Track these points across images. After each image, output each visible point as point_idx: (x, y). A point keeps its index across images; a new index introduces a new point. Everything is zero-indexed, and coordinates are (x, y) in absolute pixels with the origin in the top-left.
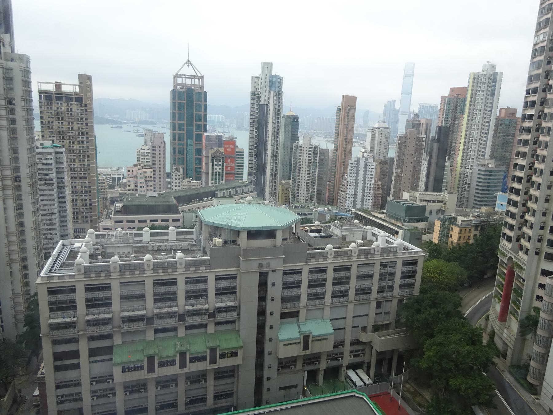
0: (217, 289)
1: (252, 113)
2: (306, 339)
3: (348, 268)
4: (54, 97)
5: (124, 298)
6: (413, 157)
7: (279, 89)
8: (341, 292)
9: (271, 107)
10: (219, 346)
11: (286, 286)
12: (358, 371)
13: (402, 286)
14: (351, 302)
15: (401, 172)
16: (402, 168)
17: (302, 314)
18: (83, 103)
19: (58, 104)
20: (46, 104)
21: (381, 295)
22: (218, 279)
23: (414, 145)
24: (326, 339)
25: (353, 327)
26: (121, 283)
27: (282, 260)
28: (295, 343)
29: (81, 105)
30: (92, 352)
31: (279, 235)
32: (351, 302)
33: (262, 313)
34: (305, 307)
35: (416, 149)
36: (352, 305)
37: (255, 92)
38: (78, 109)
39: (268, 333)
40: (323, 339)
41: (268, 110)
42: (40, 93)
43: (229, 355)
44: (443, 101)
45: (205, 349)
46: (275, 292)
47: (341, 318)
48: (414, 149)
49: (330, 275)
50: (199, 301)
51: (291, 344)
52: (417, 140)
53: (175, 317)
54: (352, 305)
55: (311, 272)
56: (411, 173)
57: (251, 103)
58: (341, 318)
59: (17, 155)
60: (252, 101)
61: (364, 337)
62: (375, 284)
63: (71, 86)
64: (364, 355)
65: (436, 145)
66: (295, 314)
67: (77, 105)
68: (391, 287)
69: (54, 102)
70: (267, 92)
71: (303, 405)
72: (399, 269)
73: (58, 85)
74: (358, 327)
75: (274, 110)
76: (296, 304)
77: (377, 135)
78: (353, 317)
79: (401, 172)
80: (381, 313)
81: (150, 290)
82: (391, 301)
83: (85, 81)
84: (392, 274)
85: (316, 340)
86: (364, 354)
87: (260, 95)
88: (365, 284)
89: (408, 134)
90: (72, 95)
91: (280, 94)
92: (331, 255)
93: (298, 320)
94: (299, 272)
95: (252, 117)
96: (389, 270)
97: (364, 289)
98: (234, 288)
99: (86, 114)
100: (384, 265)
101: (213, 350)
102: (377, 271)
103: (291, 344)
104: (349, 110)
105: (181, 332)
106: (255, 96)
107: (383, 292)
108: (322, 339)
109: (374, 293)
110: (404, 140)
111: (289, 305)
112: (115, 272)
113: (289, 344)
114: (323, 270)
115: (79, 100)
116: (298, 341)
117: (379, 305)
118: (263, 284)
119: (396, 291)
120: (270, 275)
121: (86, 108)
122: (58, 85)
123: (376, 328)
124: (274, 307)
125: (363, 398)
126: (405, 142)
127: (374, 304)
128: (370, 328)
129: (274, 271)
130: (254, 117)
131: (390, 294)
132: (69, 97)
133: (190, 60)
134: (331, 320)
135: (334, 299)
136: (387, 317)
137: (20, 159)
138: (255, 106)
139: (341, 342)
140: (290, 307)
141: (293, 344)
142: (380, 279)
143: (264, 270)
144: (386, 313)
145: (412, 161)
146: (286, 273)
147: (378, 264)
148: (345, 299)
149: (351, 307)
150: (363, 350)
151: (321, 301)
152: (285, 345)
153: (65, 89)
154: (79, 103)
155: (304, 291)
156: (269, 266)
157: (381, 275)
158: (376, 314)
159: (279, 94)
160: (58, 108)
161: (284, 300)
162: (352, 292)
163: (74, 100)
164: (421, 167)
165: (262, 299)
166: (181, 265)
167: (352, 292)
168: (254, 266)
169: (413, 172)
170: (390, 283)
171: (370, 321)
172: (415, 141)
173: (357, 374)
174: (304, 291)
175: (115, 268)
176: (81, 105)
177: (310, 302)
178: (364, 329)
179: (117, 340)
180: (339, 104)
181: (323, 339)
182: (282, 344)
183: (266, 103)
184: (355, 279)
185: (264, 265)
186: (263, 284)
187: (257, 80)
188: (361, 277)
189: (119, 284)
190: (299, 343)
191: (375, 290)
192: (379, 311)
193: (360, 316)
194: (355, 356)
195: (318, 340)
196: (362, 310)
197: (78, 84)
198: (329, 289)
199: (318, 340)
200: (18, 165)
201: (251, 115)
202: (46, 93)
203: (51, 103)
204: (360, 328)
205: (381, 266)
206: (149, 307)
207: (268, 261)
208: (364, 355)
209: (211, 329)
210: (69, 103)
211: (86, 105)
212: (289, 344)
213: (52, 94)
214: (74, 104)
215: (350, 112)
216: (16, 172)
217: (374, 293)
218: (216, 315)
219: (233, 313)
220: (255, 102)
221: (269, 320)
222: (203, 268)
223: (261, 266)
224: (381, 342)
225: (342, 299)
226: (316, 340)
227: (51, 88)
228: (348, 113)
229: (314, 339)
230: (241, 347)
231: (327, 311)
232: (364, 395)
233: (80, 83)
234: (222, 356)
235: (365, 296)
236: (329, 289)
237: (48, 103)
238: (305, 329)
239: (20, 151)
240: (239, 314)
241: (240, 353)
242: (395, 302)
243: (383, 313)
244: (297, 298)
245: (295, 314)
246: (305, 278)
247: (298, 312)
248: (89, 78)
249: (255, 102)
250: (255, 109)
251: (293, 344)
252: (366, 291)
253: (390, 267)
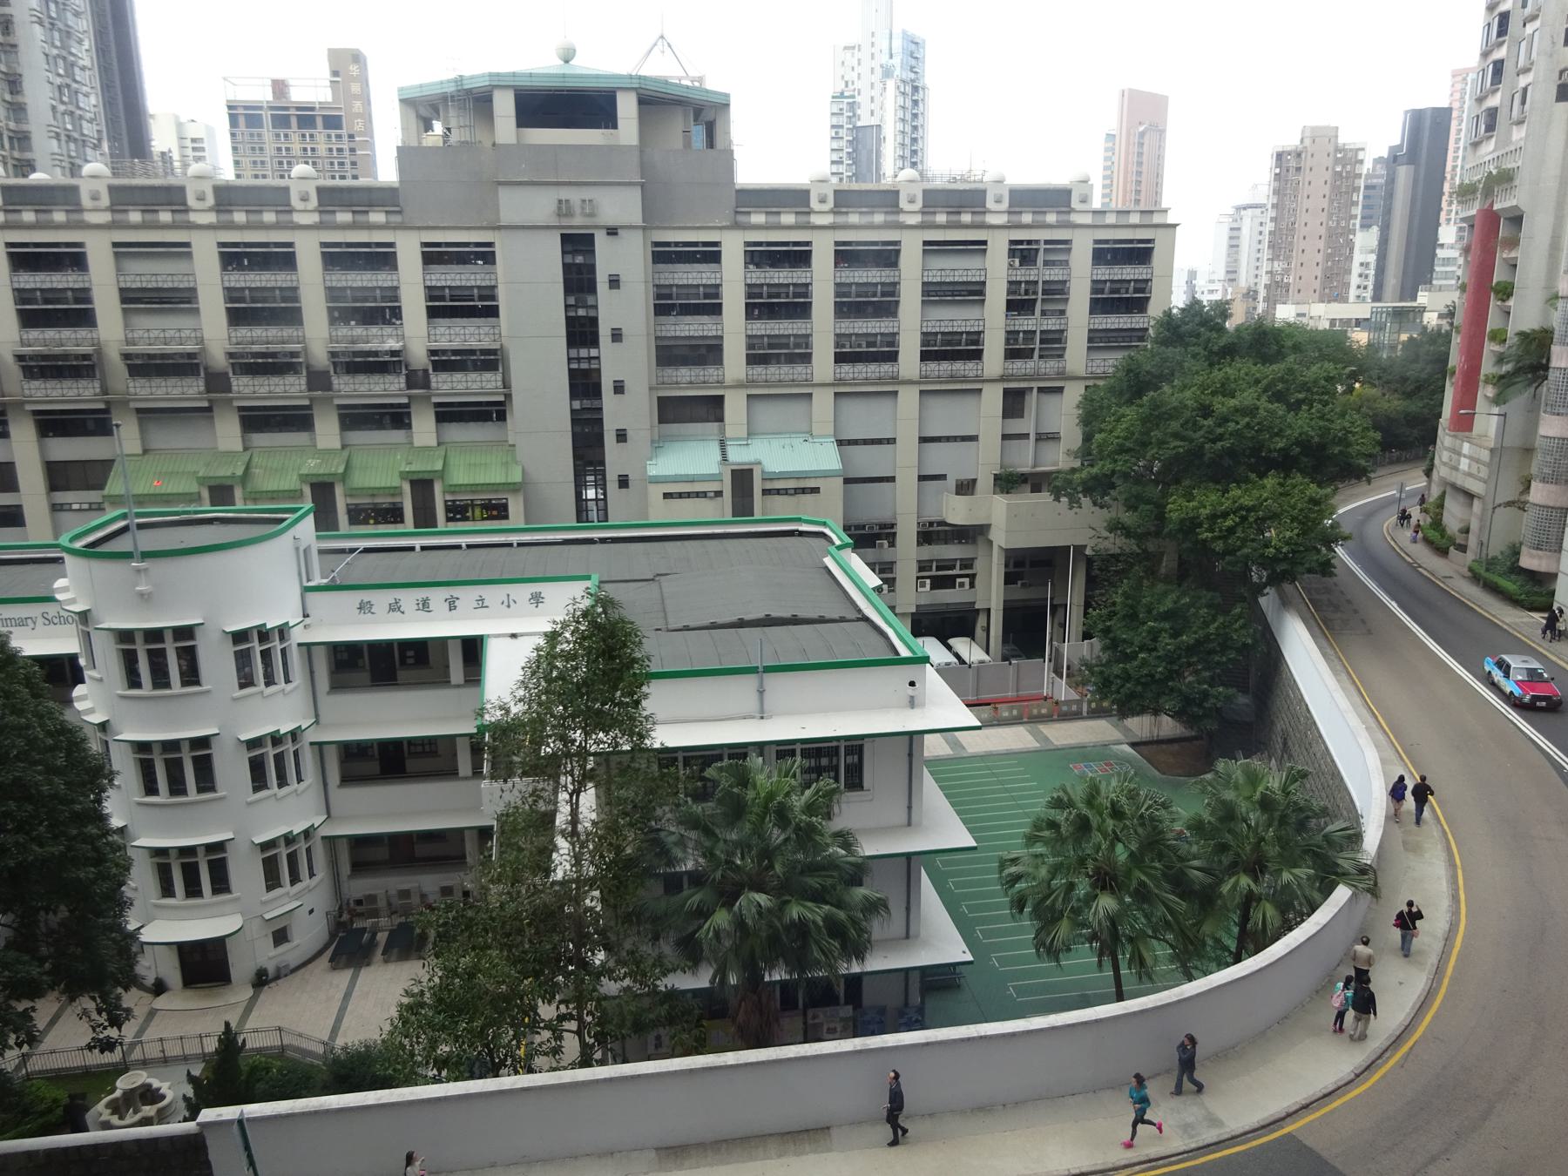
0: (432, 293)
1: (835, 158)
2: (742, 478)
3: (888, 257)
4: (267, 116)
5: (130, 298)
6: (1324, 217)
7: (913, 76)
8: (870, 339)
9: (890, 131)
10: (442, 474)
11: (666, 304)
12: (951, 641)
13: (1097, 340)
14: (910, 382)
15: (1287, 271)
16: (1288, 259)
17: (735, 406)
18: (344, 132)
19: (278, 136)
20: (247, 138)
21: (1019, 366)
22: (433, 256)
23: (1328, 176)
24: (816, 490)
25: (922, 478)
26: (115, 245)
27: (636, 195)
28: (704, 495)
29: (339, 137)
30: (59, 476)
31: (627, 107)
32: (910, 382)
33: (584, 384)
34: (739, 385)
35: (1335, 189)
36: (915, 390)
37: (842, 95)
38: (330, 150)
39: (615, 458)
40: (804, 491)
41: (880, 141)
42: (230, 107)
43: (478, 512)
44: (1459, 86)
45: (396, 482)
46: (624, 308)
47: (879, 442)
48: (1327, 190)
49: (823, 278)
50: (374, 330)
51: (689, 495)
52: (1337, 161)
53: (296, 372)
54: (915, 390)
55: (758, 257)
56: (1319, 272)
57: (833, 127)
58: (879, 442)
59: (19, 99)
60: (835, 121)
61: (957, 511)
62: (993, 320)
63: (312, 89)
64: (972, 585)
65: (1403, 172)
66: (712, 408)
67: (329, 136)
68: (1054, 342)
69: (267, 132)
70: (879, 86)
71: (603, 541)
72: (1081, 274)
73: (279, 87)
74: (942, 477)
75: (899, 139)
76: (711, 372)
77: (1245, 231)
78: (924, 440)
79: (1287, 271)
80: (1026, 436)
81: (209, 280)
82: (1060, 390)
83: (347, 66)
84: (1057, 291)
85: (778, 492)
86: (972, 577)
87: (858, 99)
88: (954, 318)
89: (1307, 142)
90: (312, 109)
91: (915, 89)
92: (823, 201)
93: (722, 431)
94: (711, 255)
95: (835, 169)
96: (1040, 273)
97: (952, 337)
98: (489, 293)
99: (354, 164)
100: (1023, 253)
101: (422, 486)
102: (997, 271)
103: (689, 495)
104: (1142, 134)
105: (327, 431)
106: (845, 102)
107: (1026, 354)
108: (803, 487)
109: (993, 358)
110: (1293, 164)
111: (685, 373)
112: (96, 210)
113: (680, 495)
114: (799, 257)
115: (333, 122)
116: (715, 487)
117: (1014, 403)
118: (579, 280)
119: (1076, 355)
120: (601, 242)
121: (352, 145)
122: (279, 87)
123: (1007, 482)
124: (626, 362)
125: (823, 535)
126: (1298, 169)
127: (993, 398)
128: (985, 483)
129: (612, 231)
130: (842, 168)
131: (1050, 366)
132: (306, 118)
133: (670, 38)
134: (840, 443)
135: (847, 370)
136: (1048, 447)
137: (31, 110)
138: (843, 132)
139: (883, 526)
140: (687, 381)
141: (698, 495)
142: (1012, 306)
143: (578, 222)
144: (1041, 438)
145: (1322, 230)
146: (663, 255)
147: (999, 246)
148: (886, 368)
149: (909, 398)
150: (967, 564)
151: (799, 370)
152: (667, 496)
153: (300, 94)
154: (333, 132)
155: (733, 327)
156: (592, 215)
157: (1013, 285)
158: (1005, 437)
159: (913, 92)
160: (279, 149)
161: (669, 354)
162: (910, 348)
163: (319, 122)
164: (1352, 250)
165: (582, 332)
166: (304, 199)
167: (910, 348)
168: (539, 206)
169: (1326, 270)
170: (1051, 324)
171: (985, 460)
172: (1329, 162)
173: (949, 648)
174: (733, 327)
175: (95, 198)
176: (339, 137)
177: (759, 370)
178: (966, 487)
179: (128, 436)
180: (1111, 123)
181: (804, 491)
182: (656, 492)
183: (874, 121)
184: (918, 297)
185: (578, 210)
186: (579, 280)
187: (848, 53)
188: (935, 293)
189: (108, 252)
190: (719, 494)
191: (994, 347)
192: (1016, 426)
193: (948, 439)
194: (940, 583)
195: (785, 492)
196: (948, 417)
197: (327, 74)
198: (823, 327)
199: (785, 492)
200: (24, 127)
201: (833, 162)
202: (246, 108)
203: (259, 135)
204: (951, 483)
205: (1012, 253)
206: (213, 331)
207: (587, 193)
208: (972, 585)
209: (424, 428)
210: (307, 132)
211: (351, 136)
212: (680, 495)
213: (261, 108)
214: (320, 133)
215: (1146, 140)
216: (22, 150)
217: (993, 358)
218: (433, 378)
219: (488, 376)
220: (843, 120)
221: (614, 412)
222: (377, 217)
223: (564, 209)
224: (1012, 522)
225: (873, 369)
226: (778, 492)
227: (265, 95)
228: (1141, 145)
229: (769, 486)
230: (514, 488)
231: (823, 402)
232: (824, 524)
233: (335, 73)
234: (457, 512)
235: (959, 367)
236: (823, 327)
237: (252, 135)
238: (740, 455)
239: (27, 84)
240: (506, 384)
241: (515, 507)
242: (1074, 393)
243: (1033, 437)
244: (710, 352)
245: (712, 408)
246: (733, 278)
247: (719, 400)
248: (357, 57)
249: (843, 120)
250: (843, 144)
251: (698, 495)
252: (964, 348)
253: (1046, 263)
